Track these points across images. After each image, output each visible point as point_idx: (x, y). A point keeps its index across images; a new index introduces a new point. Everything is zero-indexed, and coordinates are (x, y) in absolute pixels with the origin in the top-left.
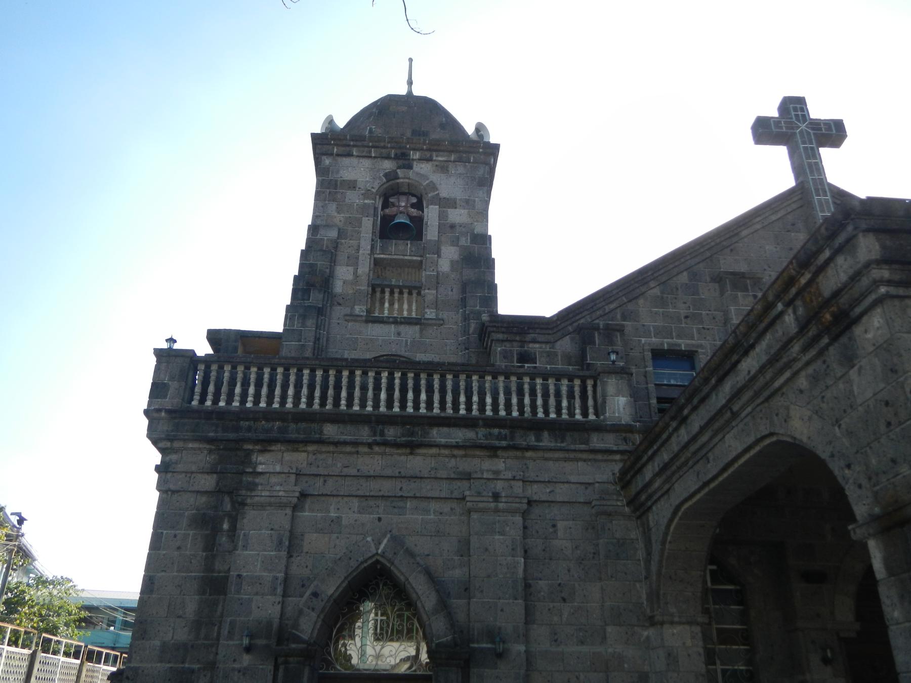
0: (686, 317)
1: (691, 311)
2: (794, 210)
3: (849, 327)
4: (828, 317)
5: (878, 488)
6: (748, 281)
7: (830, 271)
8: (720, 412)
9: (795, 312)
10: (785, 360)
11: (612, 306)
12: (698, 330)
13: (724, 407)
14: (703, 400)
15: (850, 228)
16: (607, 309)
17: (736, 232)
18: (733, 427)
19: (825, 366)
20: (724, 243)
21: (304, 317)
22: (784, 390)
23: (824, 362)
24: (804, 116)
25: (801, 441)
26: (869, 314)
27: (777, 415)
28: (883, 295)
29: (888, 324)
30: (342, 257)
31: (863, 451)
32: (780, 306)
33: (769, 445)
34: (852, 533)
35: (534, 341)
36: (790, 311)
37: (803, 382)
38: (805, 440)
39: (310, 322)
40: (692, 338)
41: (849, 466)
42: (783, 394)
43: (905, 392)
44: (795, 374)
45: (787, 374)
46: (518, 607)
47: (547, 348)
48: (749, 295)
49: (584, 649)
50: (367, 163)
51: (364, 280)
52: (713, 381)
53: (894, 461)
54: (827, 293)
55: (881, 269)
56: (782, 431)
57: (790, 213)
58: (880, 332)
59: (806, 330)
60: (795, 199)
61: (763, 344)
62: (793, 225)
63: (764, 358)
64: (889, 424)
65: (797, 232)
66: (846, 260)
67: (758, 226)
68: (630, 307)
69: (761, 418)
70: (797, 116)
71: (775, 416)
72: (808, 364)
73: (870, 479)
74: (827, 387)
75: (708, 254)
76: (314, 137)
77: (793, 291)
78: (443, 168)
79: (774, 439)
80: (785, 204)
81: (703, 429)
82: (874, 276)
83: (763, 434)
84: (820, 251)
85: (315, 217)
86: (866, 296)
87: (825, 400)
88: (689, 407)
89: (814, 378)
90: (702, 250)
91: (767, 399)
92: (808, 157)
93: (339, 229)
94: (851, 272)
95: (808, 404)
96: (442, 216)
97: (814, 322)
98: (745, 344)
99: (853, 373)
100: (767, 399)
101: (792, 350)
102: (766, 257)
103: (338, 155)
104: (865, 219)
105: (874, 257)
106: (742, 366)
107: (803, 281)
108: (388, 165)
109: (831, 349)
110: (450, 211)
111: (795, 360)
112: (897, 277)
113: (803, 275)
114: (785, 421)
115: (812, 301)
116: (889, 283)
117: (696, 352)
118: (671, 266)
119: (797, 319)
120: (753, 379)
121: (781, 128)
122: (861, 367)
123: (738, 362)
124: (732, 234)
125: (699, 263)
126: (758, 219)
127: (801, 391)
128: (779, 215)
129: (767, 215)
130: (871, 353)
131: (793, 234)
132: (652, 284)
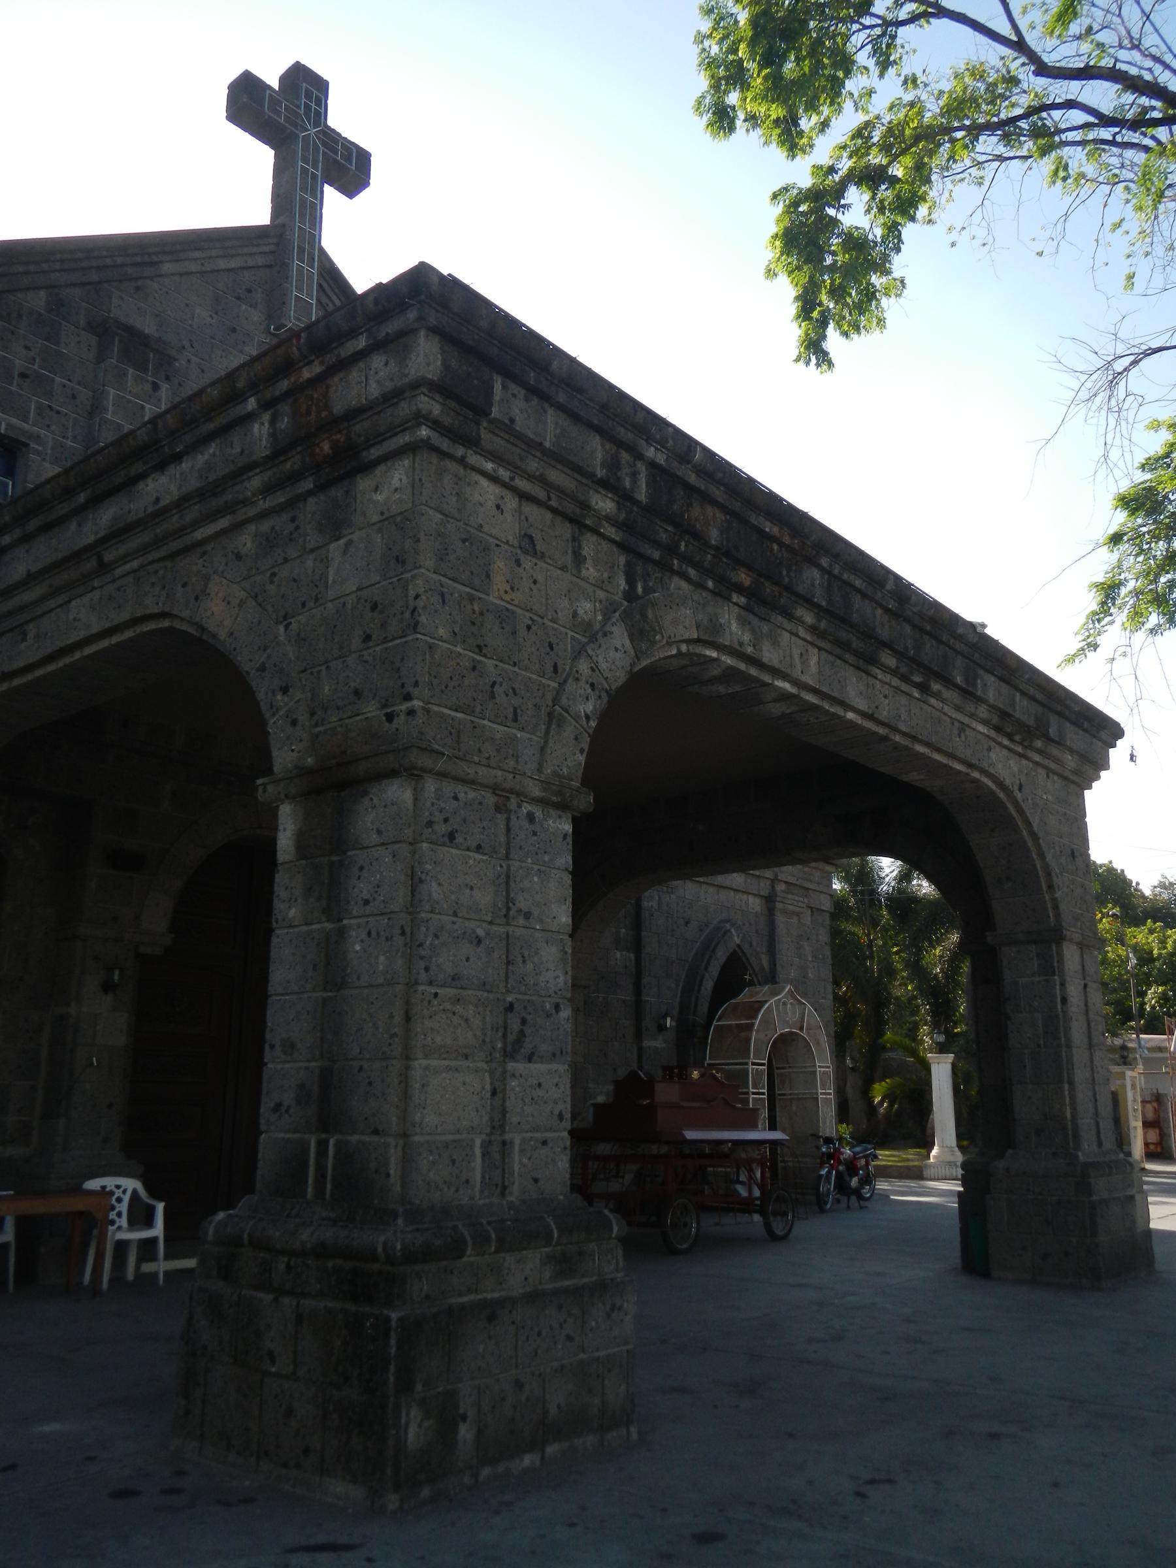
0: (23, 375)
1: (36, 367)
2: (259, 267)
3: (351, 474)
4: (326, 447)
5: (321, 729)
6: (152, 355)
7: (355, 374)
8: (76, 557)
9: (273, 421)
10: (229, 497)
12: (40, 410)
13: (88, 548)
14: (48, 527)
15: (412, 315)
17: (154, 258)
18: (94, 588)
19: (292, 526)
20: (129, 270)
22: (209, 547)
23: (293, 519)
24: (318, 114)
25: (214, 636)
26: (389, 464)
27: (184, 585)
28: (422, 440)
29: (413, 487)
31: (315, 670)
32: (252, 403)
33: (152, 632)
34: (260, 790)
36: (266, 417)
37: (246, 541)
38: (223, 635)
40: (25, 418)
41: (285, 690)
42: (205, 553)
43: (407, 596)
44: (237, 526)
45: (224, 523)
48: (148, 381)
52: (82, 498)
53: (357, 693)
54: (339, 408)
55: (432, 398)
56: (185, 614)
57: (250, 267)
58: (397, 496)
59: (282, 458)
60: (266, 249)
61: (200, 459)
62: (249, 291)
63: (194, 484)
64: (368, 638)
65: (251, 306)
66: (386, 364)
67: (194, 267)
69: (153, 584)
70: (308, 107)
71: (179, 585)
72: (263, 515)
73: (313, 714)
74: (286, 560)
75: (95, 277)
77: (284, 385)
79: (166, 623)
80: (246, 250)
81: (31, 578)
82: (421, 406)
83: (149, 612)
84: (352, 334)
86: (396, 434)
87: (276, 579)
88: (17, 533)
89: (267, 540)
90: (85, 264)
91: (173, 556)
92: (304, 189)
94: (389, 386)
95: (244, 579)
97: (299, 449)
98: (166, 449)
99: (336, 548)
100: (173, 556)
101: (246, 484)
102: (190, 325)
104: (437, 311)
105: (430, 376)
106: (147, 485)
107: (306, 374)
109: (311, 500)
111: (245, 502)
112: (447, 420)
113: (310, 363)
114: (197, 598)
115: (308, 412)
116: (436, 425)
117: (26, 445)
118: (21, 269)
119: (273, 435)
120: (161, 513)
121: (279, 113)
122: (350, 542)
123: (142, 476)
124: (147, 259)
125: (75, 285)
126: (197, 254)
127: (238, 557)
128: (234, 263)
129: (214, 253)
130: (374, 524)
131: (244, 307)
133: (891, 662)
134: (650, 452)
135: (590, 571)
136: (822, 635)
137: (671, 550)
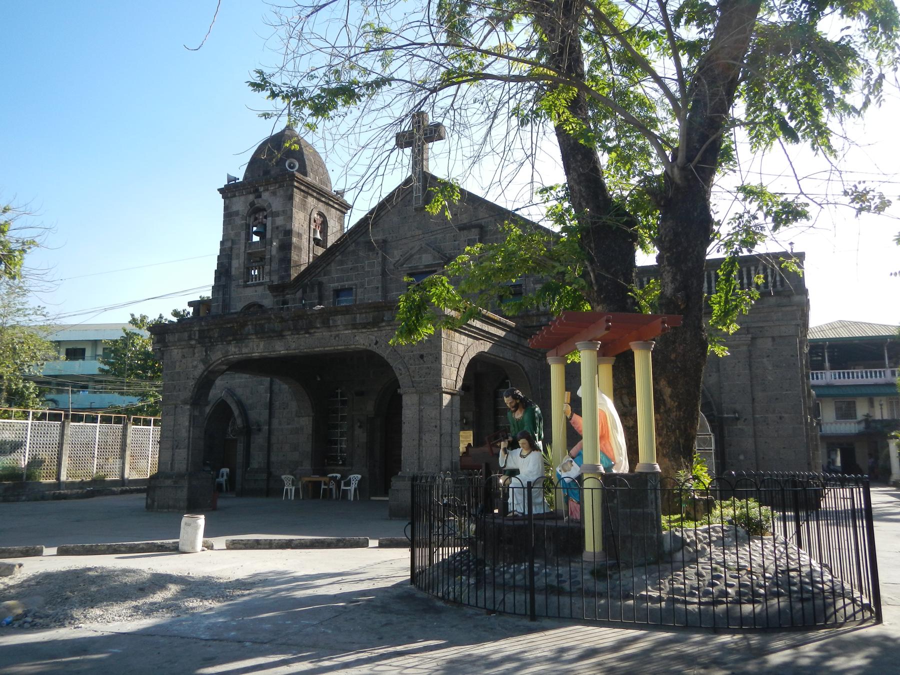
16: (317, 272)
21: (218, 291)
30: (234, 256)
35: (288, 294)
39: (221, 293)
46: (265, 413)
47: (293, 296)
49: (289, 426)
50: (243, 198)
51: (242, 265)
68: (328, 268)
75: (364, 231)
76: (221, 191)
78: (274, 193)
85: (223, 236)
93: (232, 240)
96: (273, 222)
108: (251, 197)
110: (277, 218)
133: (290, 333)
134: (195, 329)
135: (197, 355)
136: (262, 338)
137: (211, 342)
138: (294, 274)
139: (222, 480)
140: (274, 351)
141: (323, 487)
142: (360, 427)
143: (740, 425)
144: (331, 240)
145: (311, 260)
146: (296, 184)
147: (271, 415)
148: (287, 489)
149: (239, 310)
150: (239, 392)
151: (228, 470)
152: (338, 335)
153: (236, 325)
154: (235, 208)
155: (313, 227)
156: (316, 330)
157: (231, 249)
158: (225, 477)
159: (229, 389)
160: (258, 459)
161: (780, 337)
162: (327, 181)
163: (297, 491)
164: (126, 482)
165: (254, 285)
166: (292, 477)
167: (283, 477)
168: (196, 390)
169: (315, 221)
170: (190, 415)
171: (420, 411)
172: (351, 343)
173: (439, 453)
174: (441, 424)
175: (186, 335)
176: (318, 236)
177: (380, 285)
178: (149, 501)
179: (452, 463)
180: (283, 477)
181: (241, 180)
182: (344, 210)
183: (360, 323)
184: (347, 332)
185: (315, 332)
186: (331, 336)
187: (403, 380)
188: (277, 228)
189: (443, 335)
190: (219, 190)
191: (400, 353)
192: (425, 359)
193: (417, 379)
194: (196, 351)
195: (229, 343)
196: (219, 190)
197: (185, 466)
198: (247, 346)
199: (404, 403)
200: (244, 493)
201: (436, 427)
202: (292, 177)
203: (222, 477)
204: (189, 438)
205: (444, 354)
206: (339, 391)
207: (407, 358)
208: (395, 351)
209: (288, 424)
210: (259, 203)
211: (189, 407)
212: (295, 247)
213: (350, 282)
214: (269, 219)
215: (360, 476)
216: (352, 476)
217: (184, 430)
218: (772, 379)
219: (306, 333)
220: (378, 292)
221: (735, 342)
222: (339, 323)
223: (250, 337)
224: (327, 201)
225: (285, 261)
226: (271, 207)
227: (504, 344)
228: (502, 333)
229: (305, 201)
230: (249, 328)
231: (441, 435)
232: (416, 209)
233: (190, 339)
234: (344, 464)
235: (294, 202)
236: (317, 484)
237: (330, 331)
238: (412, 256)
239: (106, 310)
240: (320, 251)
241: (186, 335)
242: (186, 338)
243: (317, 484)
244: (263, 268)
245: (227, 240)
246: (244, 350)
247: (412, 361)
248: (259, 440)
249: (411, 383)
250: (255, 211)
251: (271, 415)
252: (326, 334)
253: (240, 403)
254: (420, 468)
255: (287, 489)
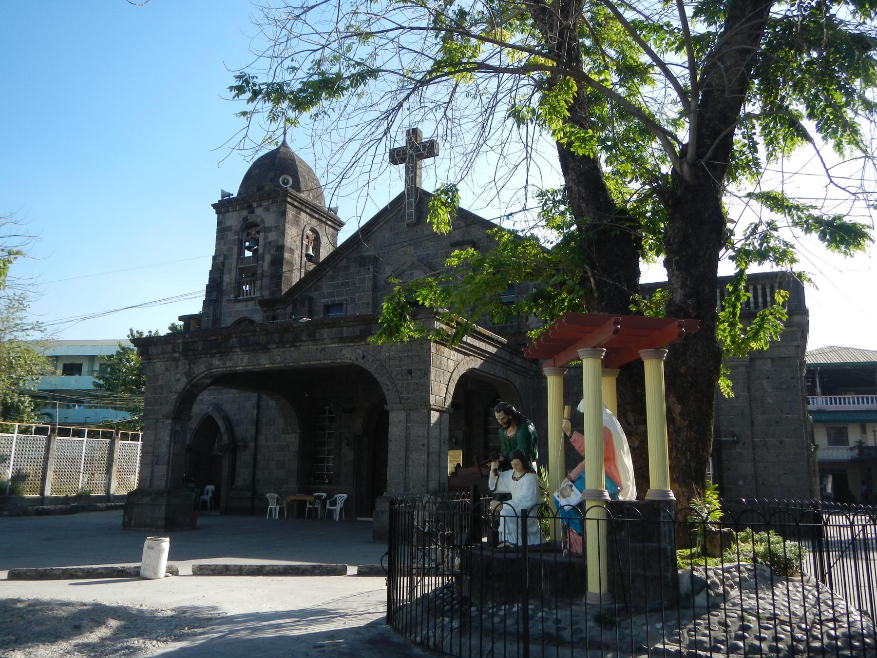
11: (310, 285)
16: (308, 287)
30: (226, 271)
35: (278, 309)
39: (211, 308)
50: (236, 214)
51: (234, 280)
67: (382, 223)
75: (356, 246)
76: (215, 206)
78: (267, 209)
96: (266, 238)
103: (224, 212)
108: (244, 213)
132: (328, 269)
133: (275, 346)
134: (179, 341)
135: (180, 368)
138: (285, 289)
139: (207, 497)
140: (259, 365)
141: (308, 506)
142: (347, 445)
143: (738, 449)
144: (324, 254)
145: (303, 276)
146: (289, 199)
147: (257, 432)
148: (271, 509)
149: (229, 325)
150: (226, 407)
151: (213, 487)
152: (324, 349)
153: (220, 337)
154: (228, 223)
155: (305, 243)
156: (303, 344)
157: (223, 264)
158: (210, 495)
159: (215, 405)
160: (243, 478)
161: (781, 358)
162: (320, 196)
163: (281, 509)
164: (112, 497)
165: (245, 300)
166: (276, 495)
167: (268, 495)
168: (178, 404)
169: (307, 237)
170: (171, 430)
171: (407, 428)
172: (338, 357)
173: (426, 473)
174: (428, 442)
175: (170, 347)
176: (311, 252)
177: (370, 301)
178: (126, 520)
179: (440, 483)
180: (268, 495)
181: (235, 195)
182: (337, 227)
183: (347, 337)
184: (333, 345)
185: (301, 346)
186: (317, 349)
187: (390, 396)
188: (270, 243)
189: (433, 350)
190: (212, 205)
191: (387, 367)
192: (413, 374)
193: (404, 395)
194: (180, 363)
195: (213, 356)
196: (212, 205)
197: (164, 483)
198: (231, 360)
199: (391, 420)
200: (227, 511)
201: (423, 445)
202: (286, 194)
203: (207, 494)
204: (169, 454)
205: (433, 370)
206: (327, 408)
207: (394, 373)
208: (383, 366)
209: (275, 441)
210: (252, 218)
211: (170, 421)
212: (287, 262)
213: (341, 298)
214: (262, 234)
215: (346, 496)
216: (338, 496)
217: (164, 446)
218: (772, 402)
219: (291, 347)
220: (368, 308)
221: (733, 363)
222: (325, 336)
223: (234, 350)
224: (320, 218)
225: (277, 276)
226: (264, 222)
227: (495, 360)
228: (493, 350)
229: (298, 217)
230: (234, 340)
231: (429, 455)
232: (408, 225)
233: (174, 351)
234: (330, 483)
235: (287, 218)
236: (302, 503)
237: (316, 345)
238: (403, 272)
239: (84, 319)
240: (312, 266)
241: (170, 347)
242: (170, 351)
243: (302, 503)
244: (255, 283)
245: (219, 255)
246: (229, 364)
247: (399, 377)
248: (245, 457)
249: (398, 400)
250: (248, 226)
251: (257, 432)
252: (312, 347)
253: (227, 419)
254: (406, 488)
255: (271, 509)
